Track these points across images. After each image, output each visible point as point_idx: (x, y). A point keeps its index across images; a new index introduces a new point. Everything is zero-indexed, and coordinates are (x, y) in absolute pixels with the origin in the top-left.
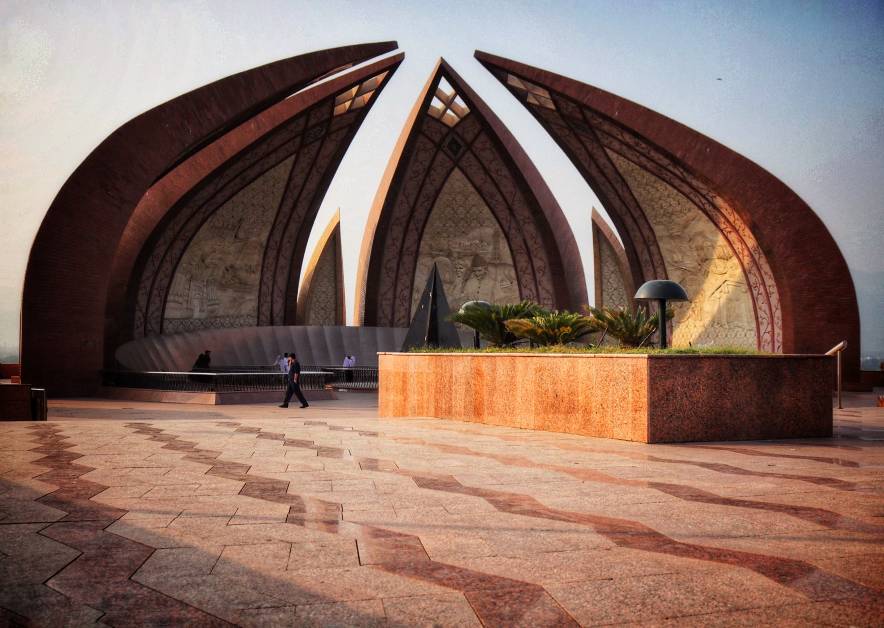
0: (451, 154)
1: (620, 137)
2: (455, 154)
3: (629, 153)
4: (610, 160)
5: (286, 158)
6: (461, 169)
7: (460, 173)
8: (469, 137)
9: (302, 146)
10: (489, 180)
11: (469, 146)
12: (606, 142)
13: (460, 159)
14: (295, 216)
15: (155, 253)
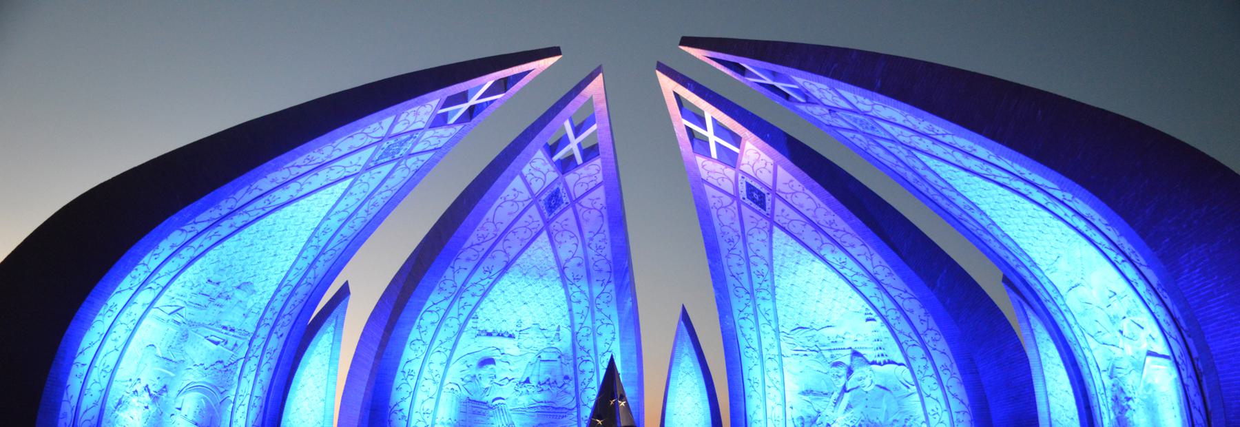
0: (758, 208)
1: (908, 124)
2: (763, 207)
3: (938, 150)
4: (934, 172)
5: (534, 239)
6: (783, 229)
7: (784, 234)
8: (767, 178)
9: (547, 223)
10: (826, 240)
11: (773, 190)
12: (907, 140)
13: (773, 212)
14: (598, 315)
15: (406, 369)
